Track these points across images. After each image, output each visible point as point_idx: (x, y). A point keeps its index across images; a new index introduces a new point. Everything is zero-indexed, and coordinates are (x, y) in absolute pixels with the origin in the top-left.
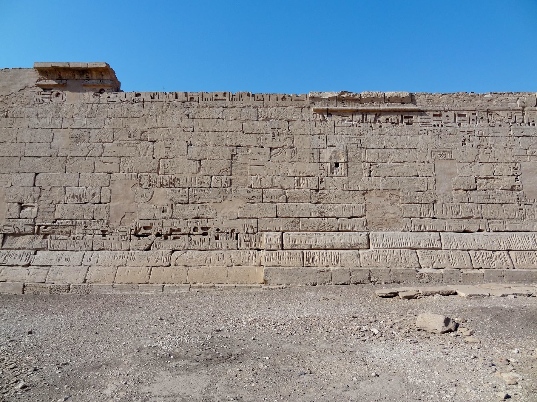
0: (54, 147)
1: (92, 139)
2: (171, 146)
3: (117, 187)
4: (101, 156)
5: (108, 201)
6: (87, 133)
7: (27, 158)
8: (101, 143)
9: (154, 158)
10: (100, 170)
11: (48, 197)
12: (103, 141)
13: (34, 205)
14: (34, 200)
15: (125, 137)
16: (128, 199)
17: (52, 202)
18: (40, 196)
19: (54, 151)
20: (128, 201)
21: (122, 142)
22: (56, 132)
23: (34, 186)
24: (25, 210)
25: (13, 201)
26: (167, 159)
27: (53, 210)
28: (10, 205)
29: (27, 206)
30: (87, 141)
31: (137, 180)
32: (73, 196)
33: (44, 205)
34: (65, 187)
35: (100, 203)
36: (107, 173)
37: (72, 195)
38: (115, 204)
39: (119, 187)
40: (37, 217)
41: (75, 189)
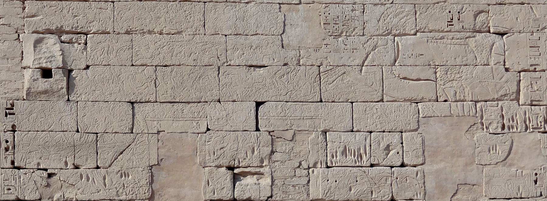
0: (289, 45)
1: (370, 28)
2: (541, 43)
3: (435, 130)
4: (394, 64)
5: (420, 161)
6: (357, 13)
7: (235, 70)
8: (390, 37)
9: (507, 70)
10: (396, 95)
11: (289, 153)
12: (394, 32)
13: (262, 170)
14: (262, 161)
15: (444, 25)
16: (460, 156)
17: (300, 164)
18: (273, 152)
19: (292, 54)
20: (462, 161)
21: (437, 35)
22: (289, 10)
23: (258, 130)
24: (242, 182)
25: (216, 163)
26: (535, 71)
27: (304, 181)
28: (210, 173)
29: (245, 174)
30: (359, 31)
31: (475, 116)
32: (344, 153)
33: (283, 170)
34: (325, 132)
35: (403, 165)
36: (411, 101)
37: (342, 149)
38: (436, 167)
39: (440, 131)
40: (271, 197)
41: (346, 137)
